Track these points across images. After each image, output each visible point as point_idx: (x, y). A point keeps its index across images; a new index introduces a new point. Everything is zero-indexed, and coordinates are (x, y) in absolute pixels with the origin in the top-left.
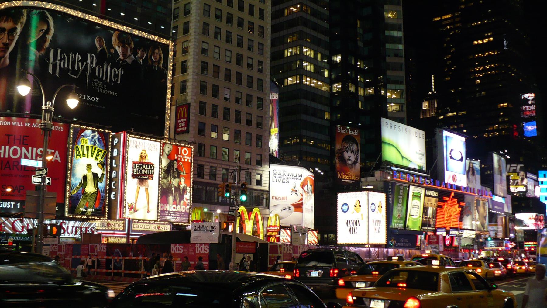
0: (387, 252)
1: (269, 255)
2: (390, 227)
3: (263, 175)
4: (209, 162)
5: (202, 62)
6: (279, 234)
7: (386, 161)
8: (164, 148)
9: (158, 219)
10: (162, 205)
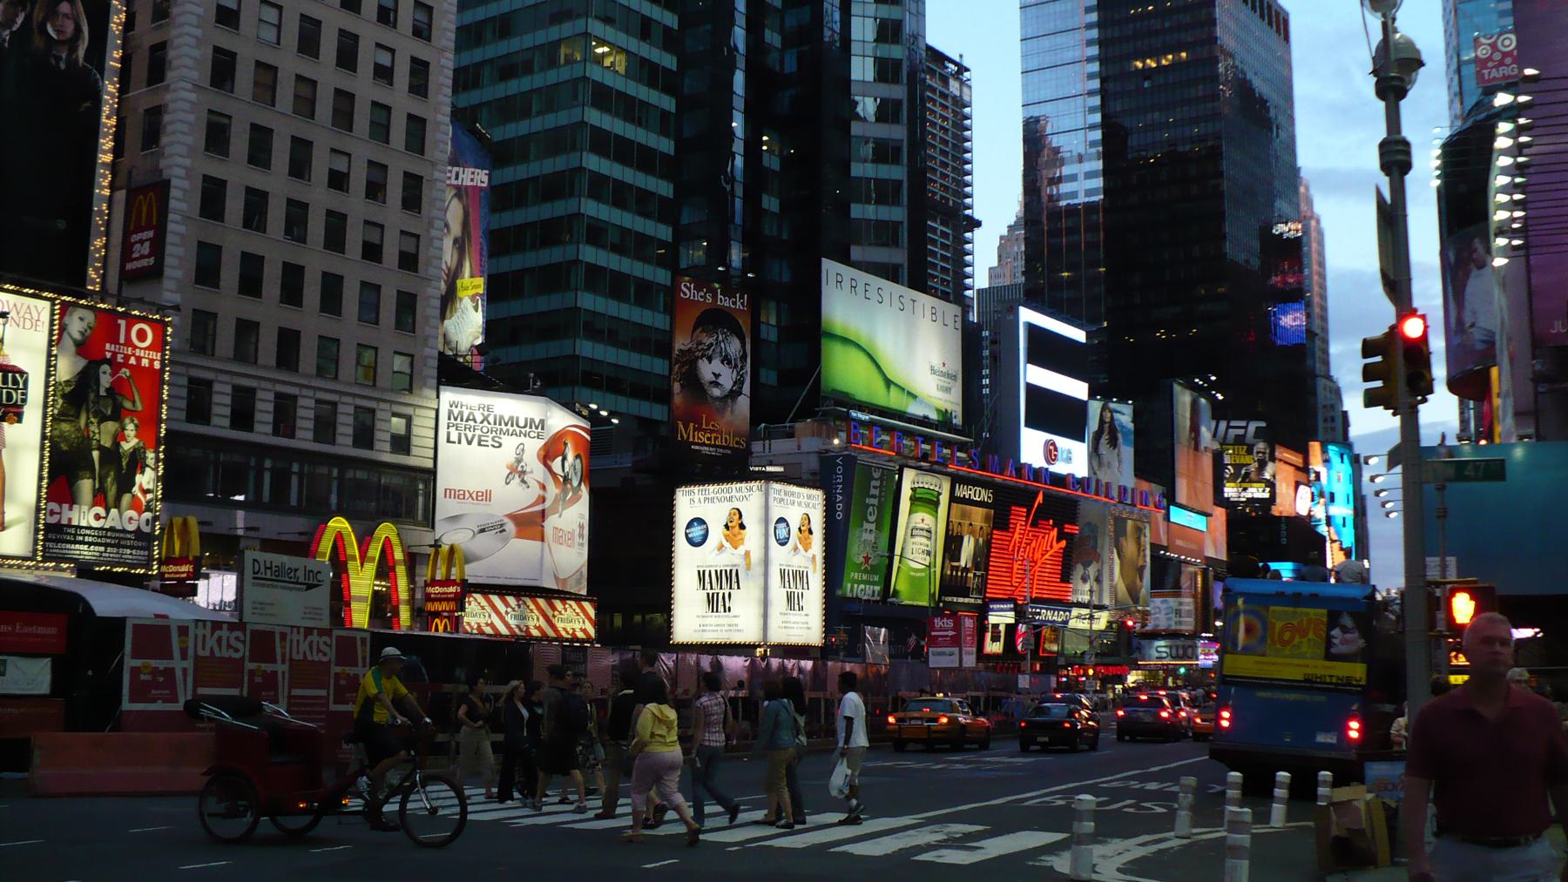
0: (698, 663)
1: (130, 663)
2: (839, 592)
3: (416, 421)
4: (269, 380)
5: (217, 50)
6: (463, 609)
7: (835, 391)
8: (66, 319)
9: (35, 551)
10: (54, 506)
